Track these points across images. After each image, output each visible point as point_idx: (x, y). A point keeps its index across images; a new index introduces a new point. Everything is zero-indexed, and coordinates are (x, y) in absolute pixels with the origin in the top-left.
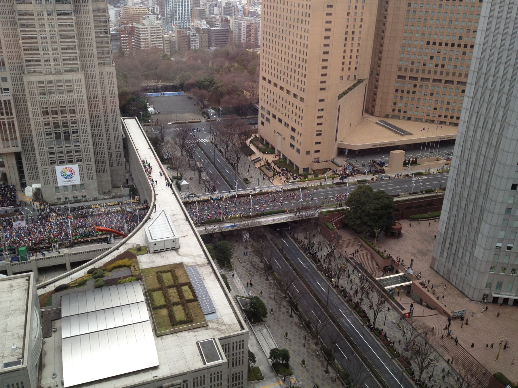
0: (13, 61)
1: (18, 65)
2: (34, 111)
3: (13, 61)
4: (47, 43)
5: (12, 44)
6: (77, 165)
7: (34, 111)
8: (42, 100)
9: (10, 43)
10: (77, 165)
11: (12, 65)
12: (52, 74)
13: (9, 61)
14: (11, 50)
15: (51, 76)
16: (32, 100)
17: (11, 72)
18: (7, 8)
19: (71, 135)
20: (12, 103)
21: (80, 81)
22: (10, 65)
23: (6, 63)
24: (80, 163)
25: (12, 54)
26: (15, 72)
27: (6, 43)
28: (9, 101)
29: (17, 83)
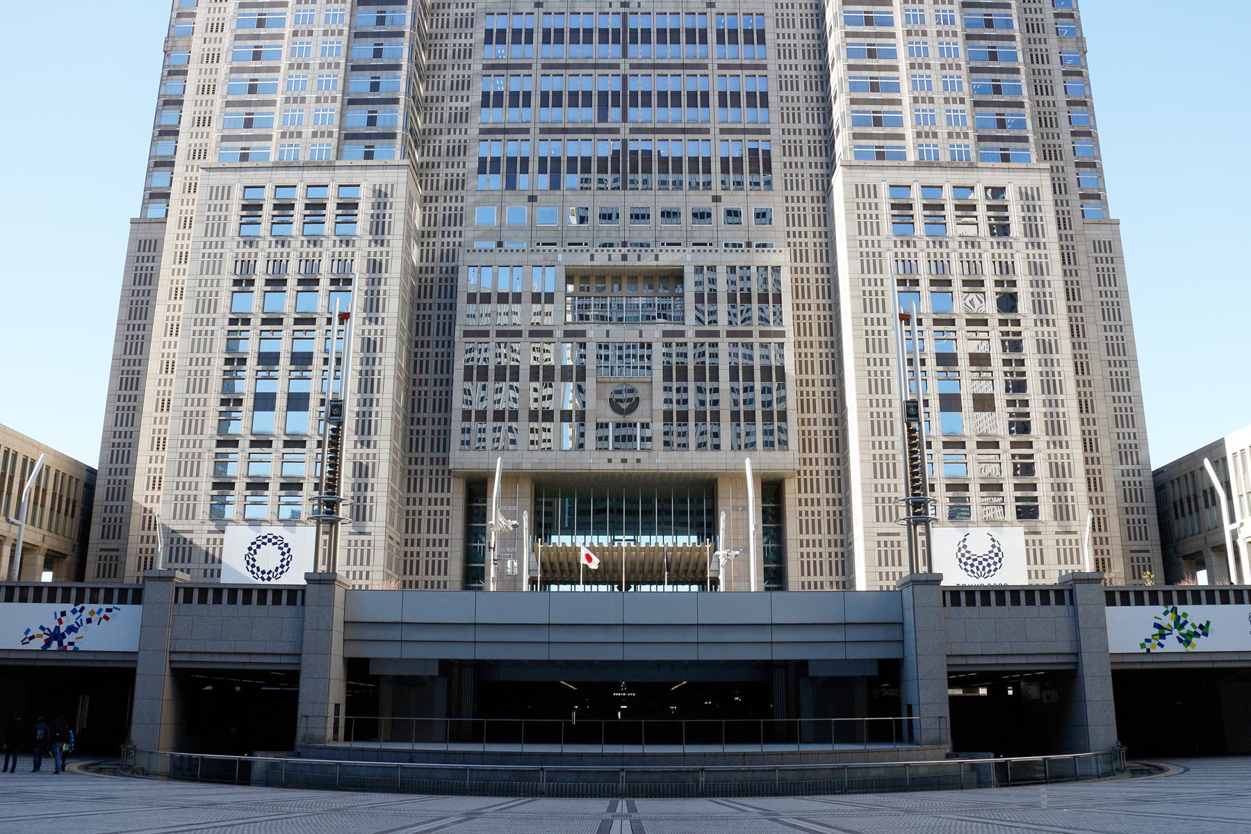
0: (799, 159)
1: (814, 171)
3: (799, 159)
4: (928, 66)
5: (803, 110)
9: (796, 105)
11: (794, 171)
12: (941, 166)
13: (787, 159)
14: (797, 126)
16: (864, 249)
20: (786, 277)
22: (788, 171)
23: (776, 165)
25: (797, 137)
27: (785, 104)
28: (777, 269)
29: (803, 229)
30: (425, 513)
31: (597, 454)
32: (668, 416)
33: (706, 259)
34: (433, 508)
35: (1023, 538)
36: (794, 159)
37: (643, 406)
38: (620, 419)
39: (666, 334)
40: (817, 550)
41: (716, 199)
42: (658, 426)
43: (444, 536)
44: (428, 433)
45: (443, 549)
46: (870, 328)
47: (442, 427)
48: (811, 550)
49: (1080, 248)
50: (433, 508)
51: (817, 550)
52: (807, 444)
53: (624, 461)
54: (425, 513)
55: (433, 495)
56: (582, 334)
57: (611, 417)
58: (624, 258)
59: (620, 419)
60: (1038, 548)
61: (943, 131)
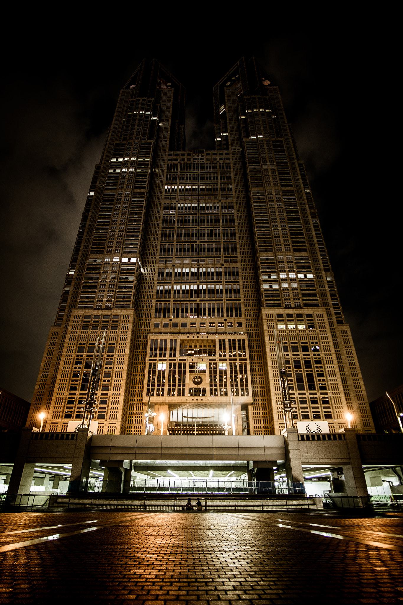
2: (271, 345)
3: (250, 308)
6: (327, 422)
7: (271, 345)
8: (281, 333)
10: (327, 422)
15: (291, 310)
16: (270, 333)
17: (247, 318)
18: (248, 266)
19: (316, 378)
20: (246, 342)
21: (322, 315)
24: (330, 420)
26: (250, 318)
28: (244, 340)
30: (134, 417)
31: (188, 398)
32: (211, 385)
33: (222, 337)
34: (137, 415)
35: (327, 425)
36: (248, 308)
37: (204, 382)
38: (196, 386)
39: (210, 360)
40: (260, 429)
41: (225, 320)
42: (208, 389)
43: (140, 425)
44: (137, 391)
45: (140, 429)
46: (273, 357)
47: (141, 389)
48: (258, 429)
49: (337, 332)
50: (137, 415)
51: (260, 429)
52: (254, 395)
53: (197, 400)
54: (134, 417)
55: (137, 411)
56: (185, 360)
57: (193, 386)
58: (198, 337)
59: (196, 386)
60: (333, 428)
61: (292, 298)
